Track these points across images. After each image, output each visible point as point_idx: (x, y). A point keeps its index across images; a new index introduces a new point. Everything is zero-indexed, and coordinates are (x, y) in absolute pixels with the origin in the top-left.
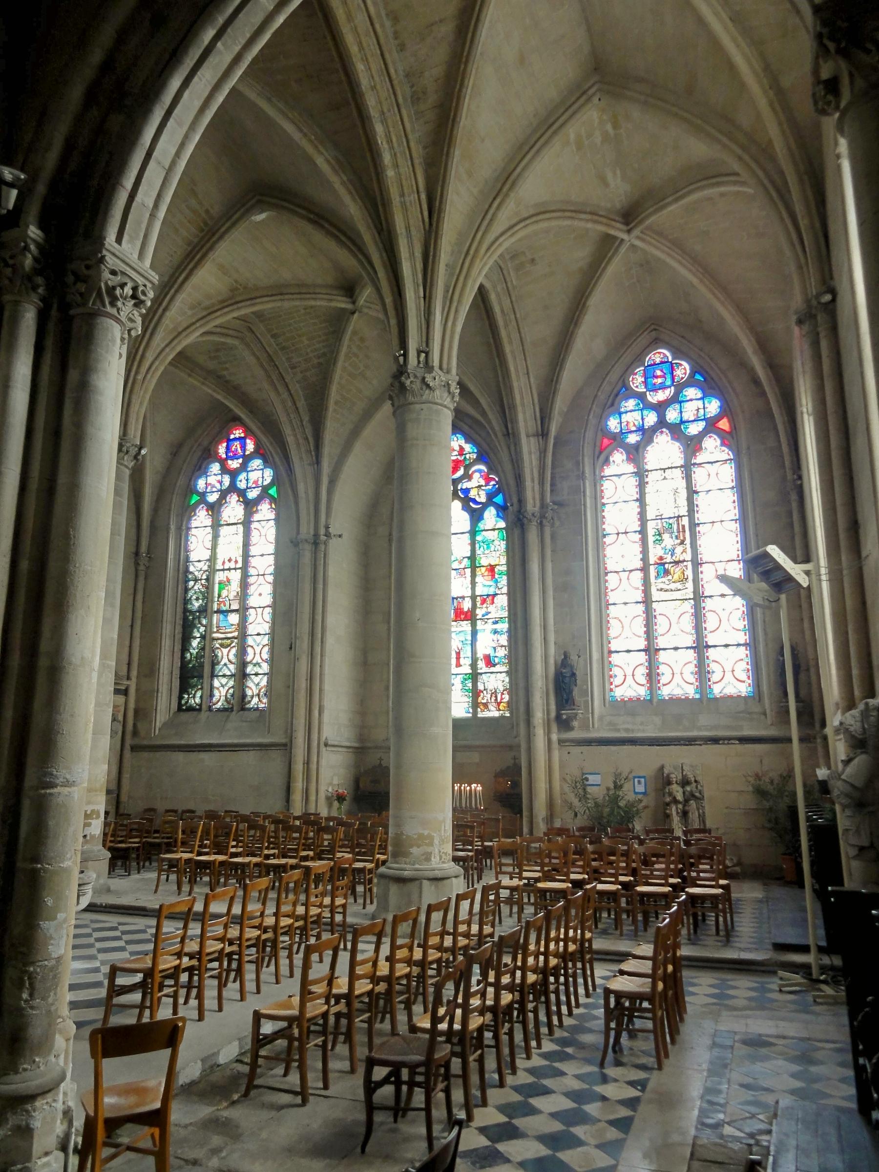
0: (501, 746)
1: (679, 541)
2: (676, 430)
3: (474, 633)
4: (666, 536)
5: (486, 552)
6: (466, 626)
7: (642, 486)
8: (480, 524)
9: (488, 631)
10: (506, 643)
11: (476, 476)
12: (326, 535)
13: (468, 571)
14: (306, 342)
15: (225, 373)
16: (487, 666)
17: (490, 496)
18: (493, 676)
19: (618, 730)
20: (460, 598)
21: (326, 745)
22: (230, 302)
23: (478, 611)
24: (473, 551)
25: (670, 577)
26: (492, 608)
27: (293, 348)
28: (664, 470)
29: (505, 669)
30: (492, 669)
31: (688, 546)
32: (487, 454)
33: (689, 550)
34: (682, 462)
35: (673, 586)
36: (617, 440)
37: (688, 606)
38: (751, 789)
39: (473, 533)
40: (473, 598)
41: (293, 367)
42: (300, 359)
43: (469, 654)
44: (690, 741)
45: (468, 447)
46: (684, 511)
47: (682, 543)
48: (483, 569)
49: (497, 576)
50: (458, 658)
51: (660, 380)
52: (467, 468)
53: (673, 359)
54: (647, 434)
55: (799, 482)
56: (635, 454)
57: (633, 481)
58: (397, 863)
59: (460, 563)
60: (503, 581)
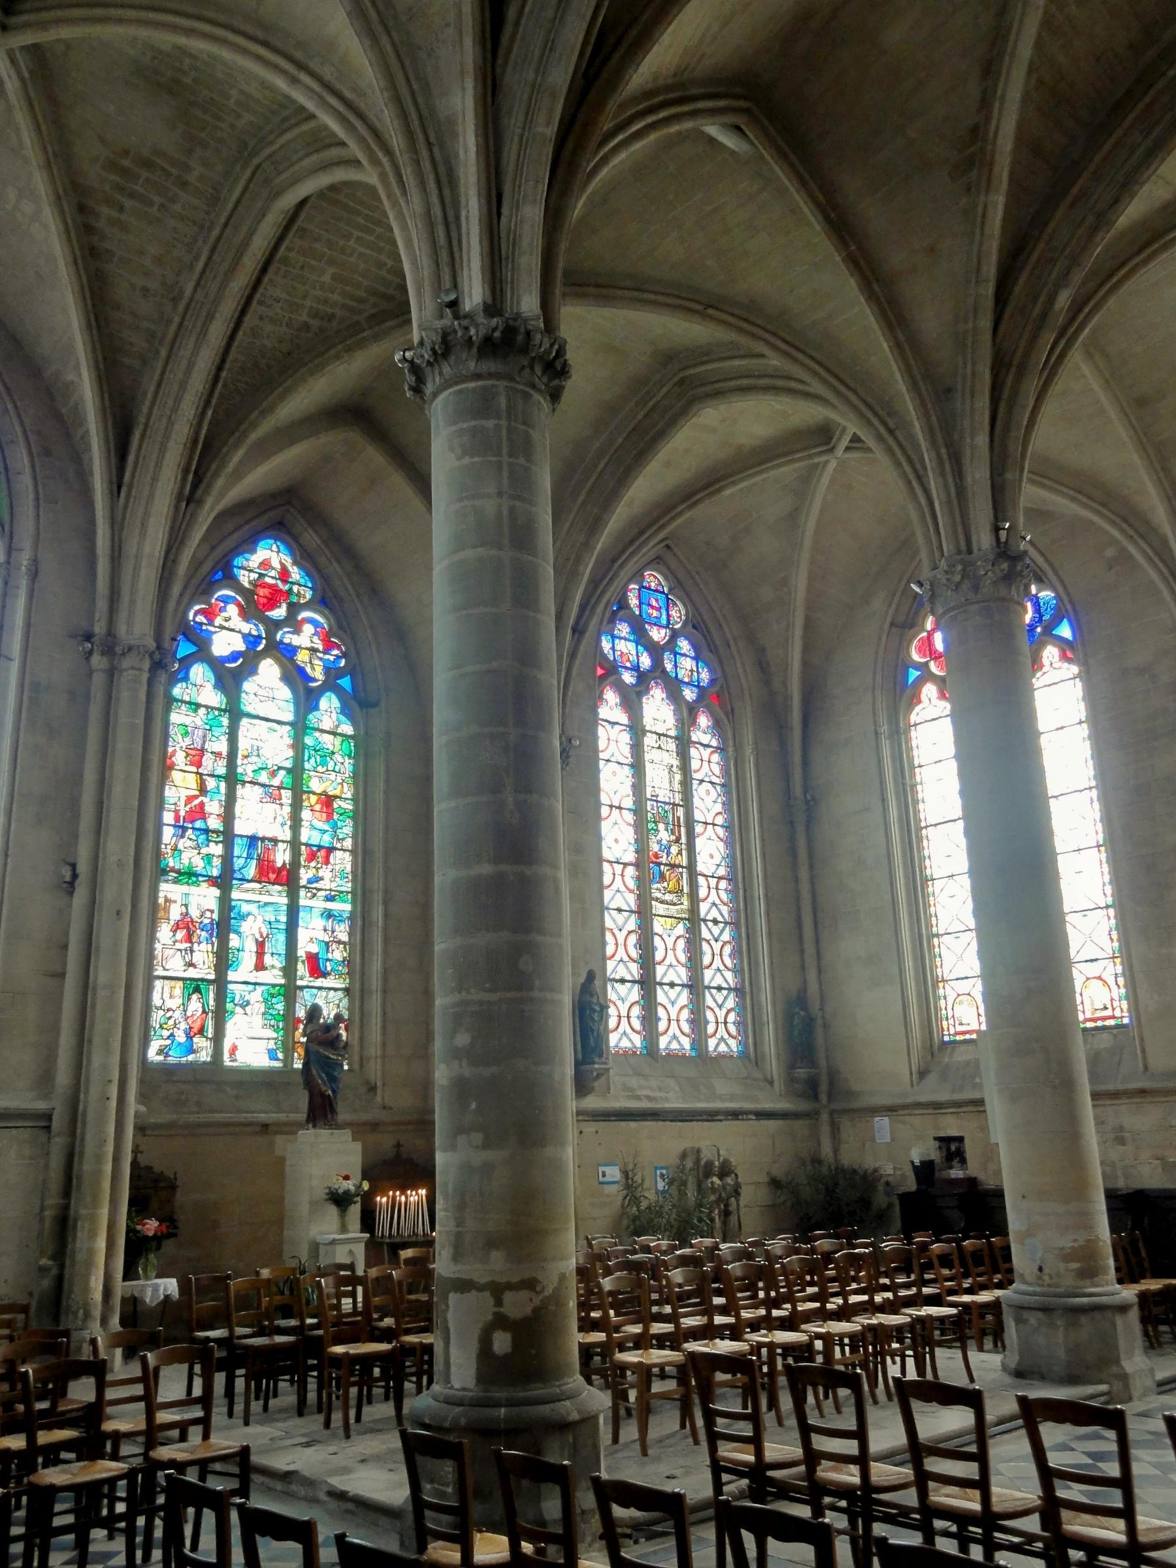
0: (365, 1124)
1: (673, 838)
2: (673, 688)
3: (293, 911)
4: (661, 826)
5: (320, 769)
6: (278, 896)
7: (637, 748)
8: (310, 717)
9: (316, 913)
10: (344, 937)
11: (308, 629)
13: (287, 795)
14: (327, 278)
15: (106, 211)
16: (312, 975)
17: (332, 673)
18: (324, 993)
19: (638, 1098)
20: (270, 840)
23: (302, 871)
24: (299, 760)
25: (665, 884)
26: (325, 872)
28: (659, 735)
29: (339, 984)
30: (320, 982)
31: (684, 846)
32: (341, 601)
33: (684, 852)
34: (673, 733)
35: (668, 897)
36: (611, 670)
37: (680, 929)
38: (764, 1178)
39: (300, 727)
40: (295, 844)
42: (284, 296)
43: (281, 948)
44: (711, 1116)
45: (296, 574)
46: (678, 799)
47: (678, 840)
48: (313, 799)
49: (336, 817)
50: (260, 954)
51: (655, 614)
52: (294, 608)
53: (670, 590)
54: (643, 678)
56: (631, 702)
57: (626, 738)
58: (1097, 1286)
59: (273, 774)
60: (347, 829)
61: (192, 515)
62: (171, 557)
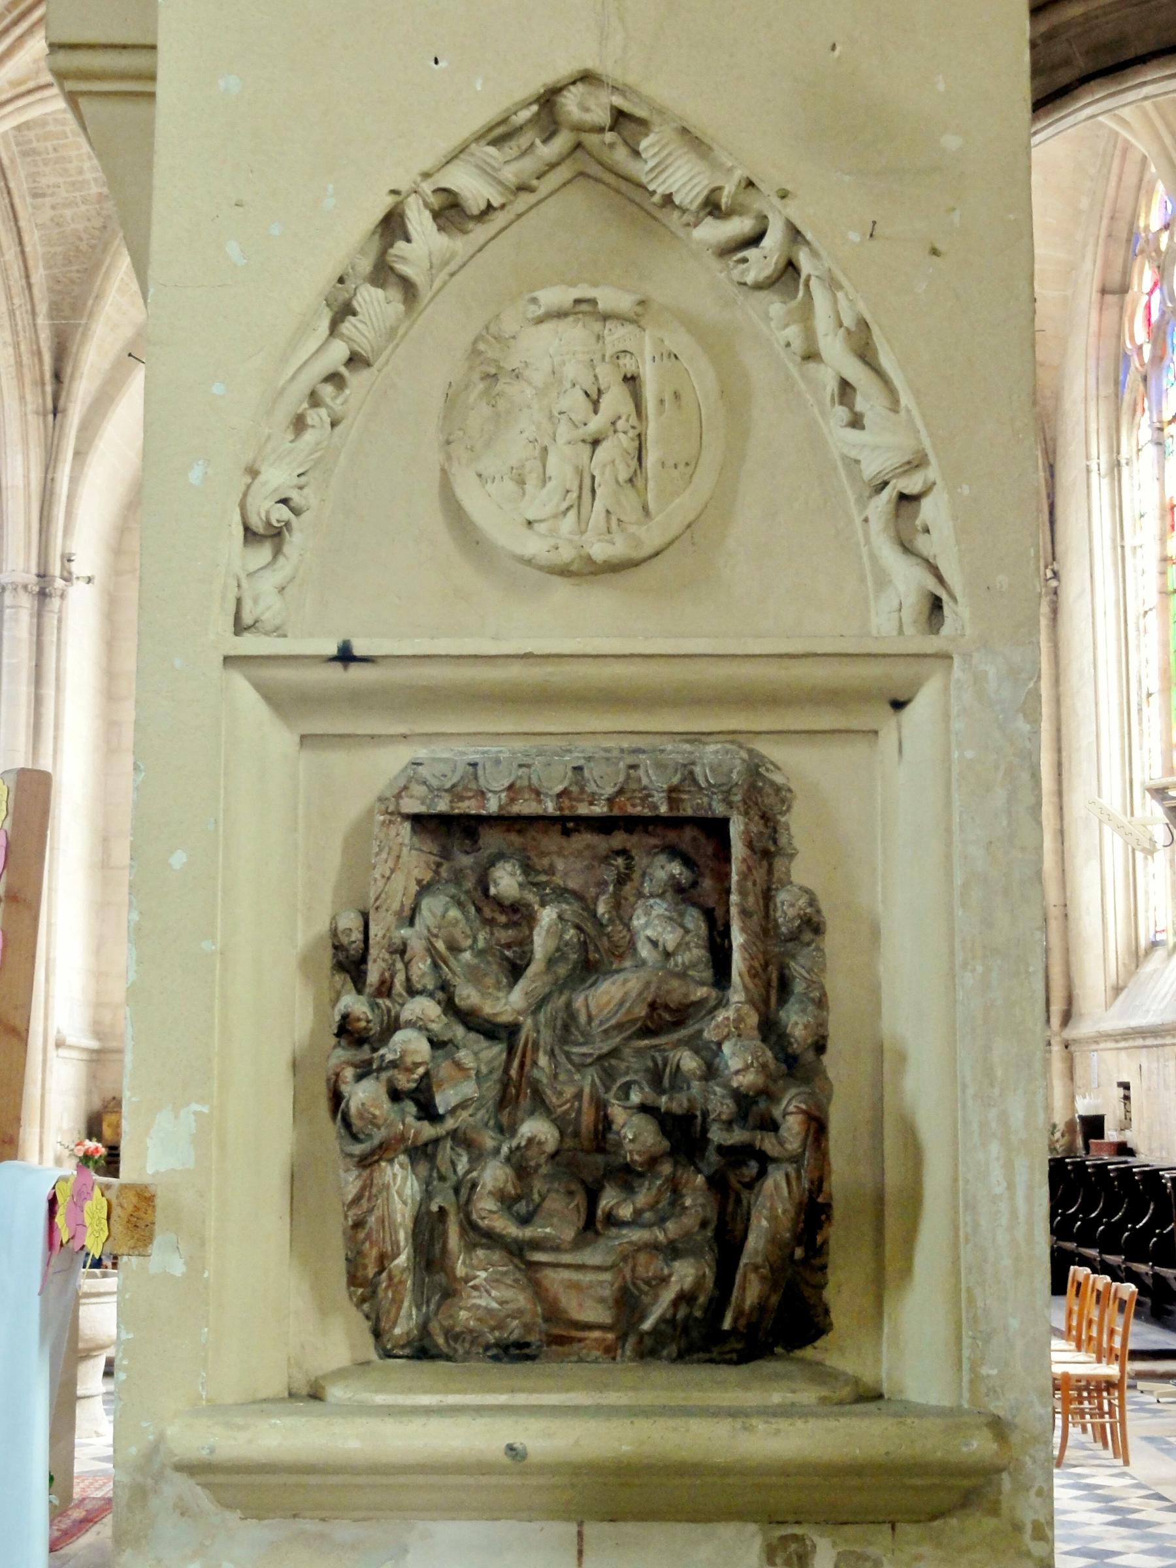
12: (63, 578)
21: (59, 1045)
22: (31, 85)
27: (52, 155)
41: (35, 195)
42: (60, 180)
55: (1054, 583)
61: (61, 427)
62: (49, 476)
